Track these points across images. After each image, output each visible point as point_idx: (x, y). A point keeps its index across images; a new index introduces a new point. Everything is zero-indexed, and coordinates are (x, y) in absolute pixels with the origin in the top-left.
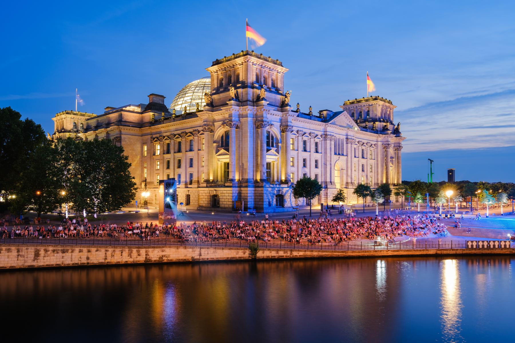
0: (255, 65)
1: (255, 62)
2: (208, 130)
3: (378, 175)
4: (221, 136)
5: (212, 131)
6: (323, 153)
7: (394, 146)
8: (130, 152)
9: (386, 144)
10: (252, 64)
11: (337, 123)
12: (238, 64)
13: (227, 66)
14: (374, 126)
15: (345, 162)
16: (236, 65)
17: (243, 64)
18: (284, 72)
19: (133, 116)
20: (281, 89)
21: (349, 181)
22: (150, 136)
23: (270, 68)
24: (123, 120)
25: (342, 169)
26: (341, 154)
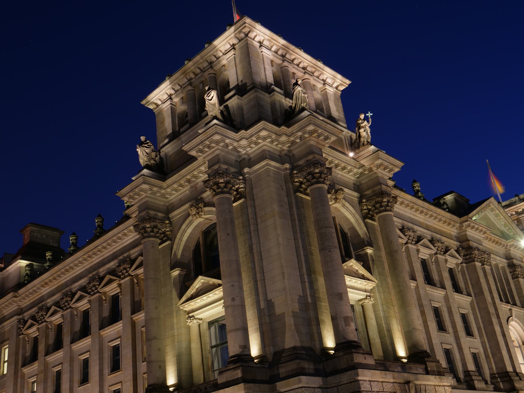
2: (152, 231)
6: (473, 295)
10: (258, 44)
22: (15, 317)
23: (304, 68)
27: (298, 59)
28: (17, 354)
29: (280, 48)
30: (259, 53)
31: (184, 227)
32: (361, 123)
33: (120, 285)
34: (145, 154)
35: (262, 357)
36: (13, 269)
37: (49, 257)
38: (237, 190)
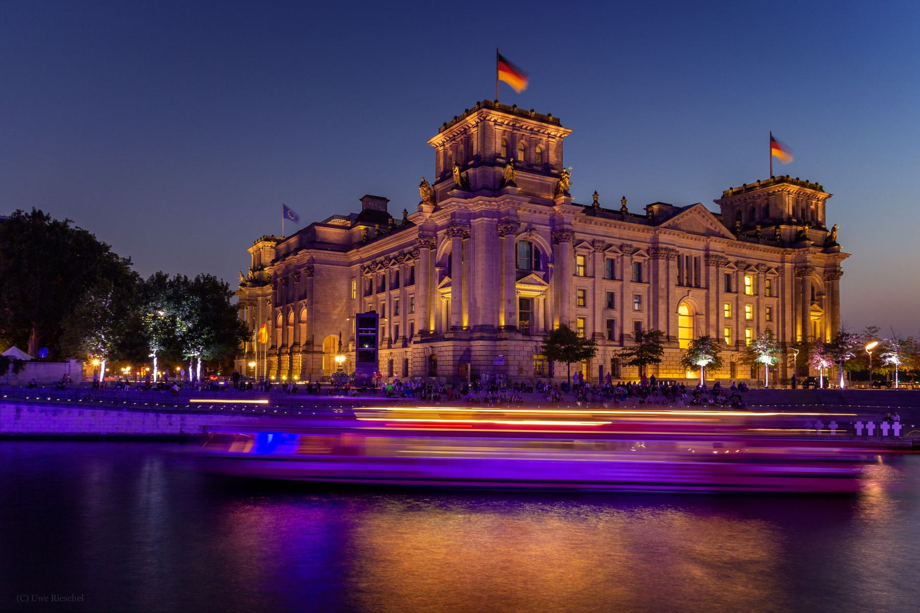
0: (501, 126)
1: (499, 121)
3: (784, 326)
4: (448, 255)
5: (434, 247)
6: (651, 282)
7: (824, 272)
8: (330, 291)
9: (801, 267)
10: (493, 123)
11: (682, 227)
12: (471, 126)
13: (456, 133)
14: (777, 233)
15: (704, 301)
16: (470, 128)
17: (479, 124)
18: (563, 136)
19: (335, 233)
20: (555, 167)
21: (713, 335)
22: (359, 265)
24: (317, 240)
25: (697, 314)
26: (693, 285)
27: (525, 125)
28: (361, 288)
29: (511, 121)
30: (493, 130)
31: (443, 243)
32: (563, 176)
33: (414, 262)
34: (423, 191)
35: (468, 327)
36: (356, 230)
37: (377, 228)
38: (466, 232)
